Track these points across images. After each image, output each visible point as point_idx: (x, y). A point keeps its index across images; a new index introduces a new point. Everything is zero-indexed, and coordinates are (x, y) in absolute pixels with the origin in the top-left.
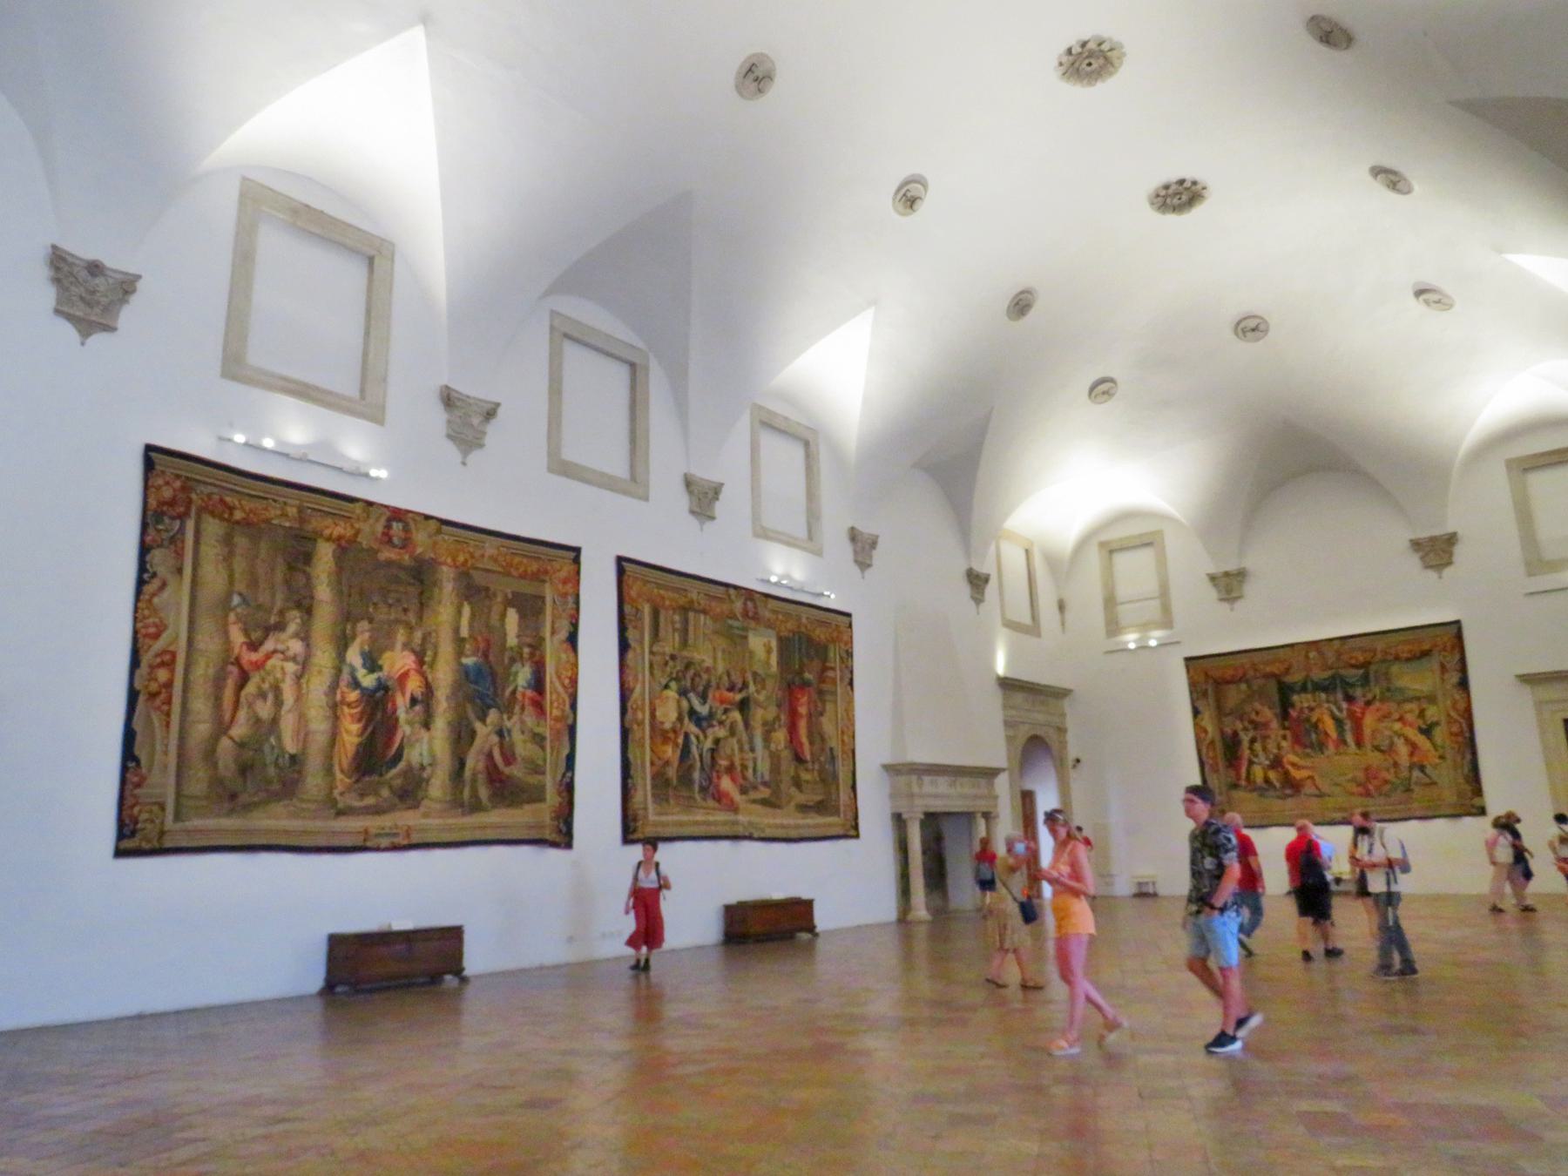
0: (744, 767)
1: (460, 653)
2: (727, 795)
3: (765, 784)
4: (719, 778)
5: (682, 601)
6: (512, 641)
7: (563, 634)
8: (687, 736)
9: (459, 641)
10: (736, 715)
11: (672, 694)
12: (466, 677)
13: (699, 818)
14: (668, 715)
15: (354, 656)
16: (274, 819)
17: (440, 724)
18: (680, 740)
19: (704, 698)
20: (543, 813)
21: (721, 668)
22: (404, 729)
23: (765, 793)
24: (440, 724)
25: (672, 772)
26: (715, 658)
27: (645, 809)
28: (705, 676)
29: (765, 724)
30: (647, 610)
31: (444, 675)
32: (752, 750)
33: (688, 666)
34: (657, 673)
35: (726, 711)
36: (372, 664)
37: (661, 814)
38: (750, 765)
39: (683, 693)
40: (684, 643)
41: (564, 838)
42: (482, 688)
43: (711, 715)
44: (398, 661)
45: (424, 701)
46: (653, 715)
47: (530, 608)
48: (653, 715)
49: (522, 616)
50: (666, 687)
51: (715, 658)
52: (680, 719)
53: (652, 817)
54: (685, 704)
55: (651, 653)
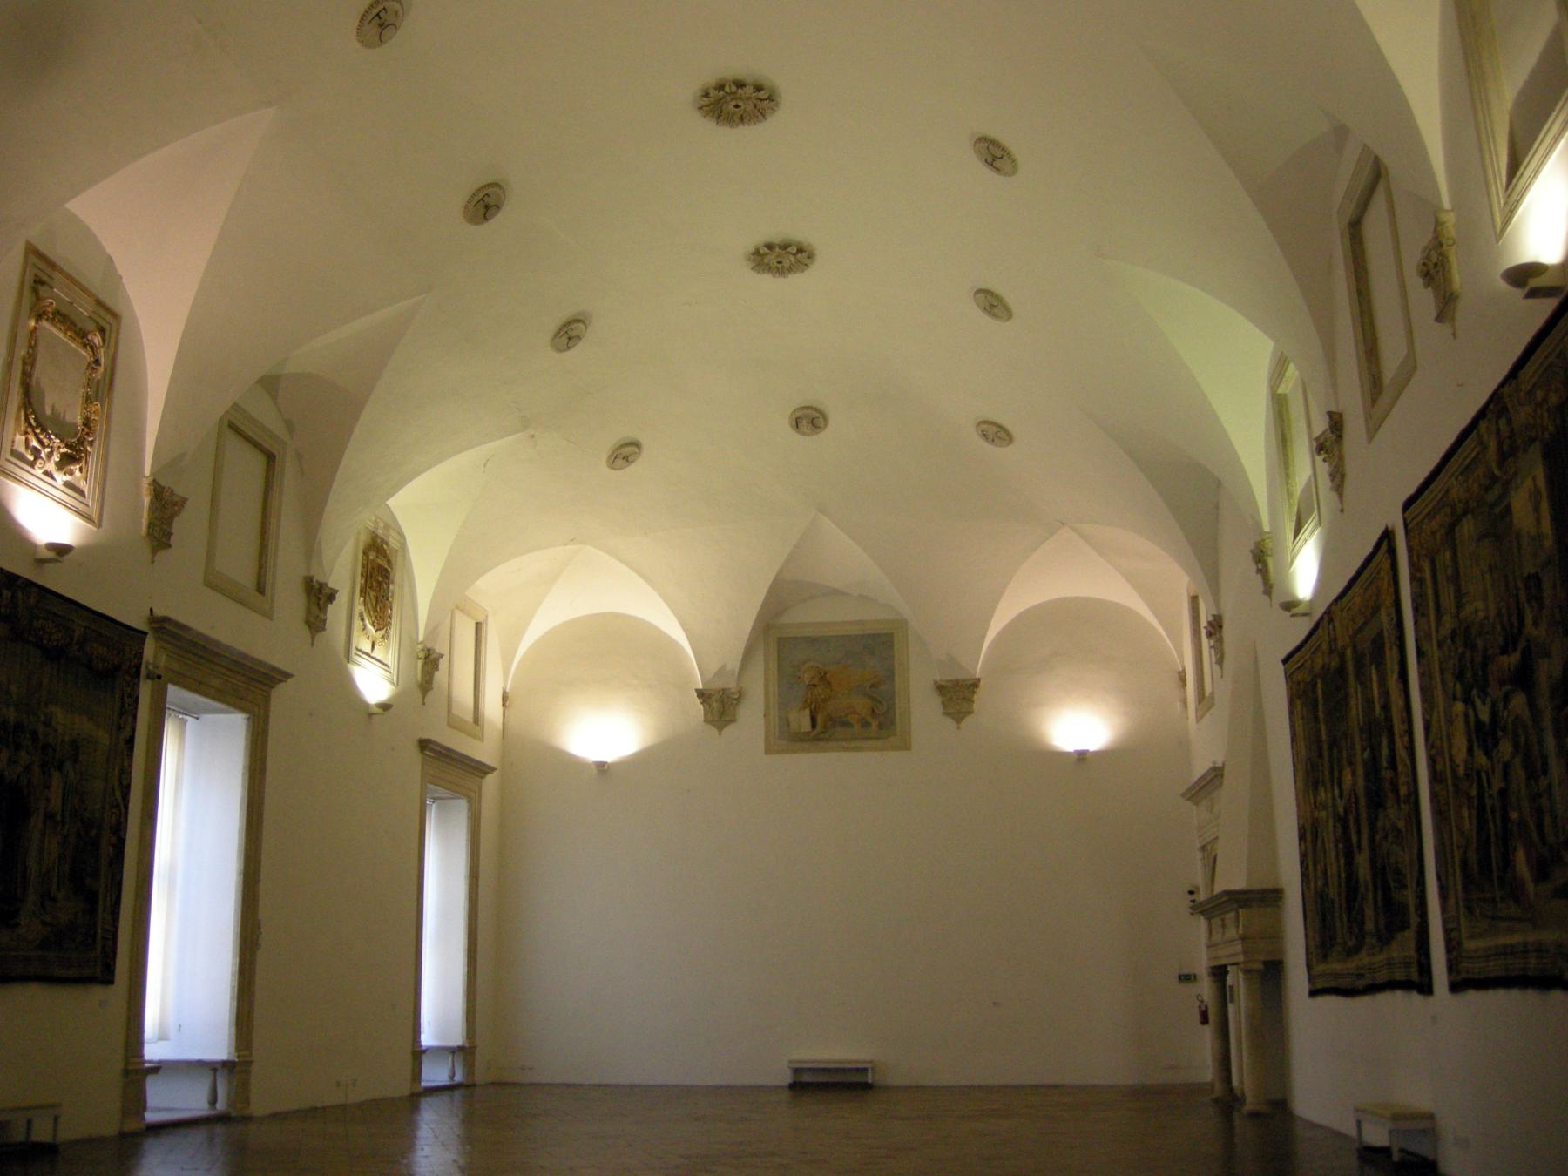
1: (1363, 750)
7: (1395, 675)
9: (1361, 730)
17: (1365, 843)
18: (1474, 793)
21: (1493, 612)
28: (1480, 643)
31: (1361, 781)
32: (1545, 772)
39: (1468, 700)
44: (1348, 778)
45: (1357, 820)
46: (1451, 760)
50: (1455, 698)
52: (1470, 751)
55: (1440, 646)
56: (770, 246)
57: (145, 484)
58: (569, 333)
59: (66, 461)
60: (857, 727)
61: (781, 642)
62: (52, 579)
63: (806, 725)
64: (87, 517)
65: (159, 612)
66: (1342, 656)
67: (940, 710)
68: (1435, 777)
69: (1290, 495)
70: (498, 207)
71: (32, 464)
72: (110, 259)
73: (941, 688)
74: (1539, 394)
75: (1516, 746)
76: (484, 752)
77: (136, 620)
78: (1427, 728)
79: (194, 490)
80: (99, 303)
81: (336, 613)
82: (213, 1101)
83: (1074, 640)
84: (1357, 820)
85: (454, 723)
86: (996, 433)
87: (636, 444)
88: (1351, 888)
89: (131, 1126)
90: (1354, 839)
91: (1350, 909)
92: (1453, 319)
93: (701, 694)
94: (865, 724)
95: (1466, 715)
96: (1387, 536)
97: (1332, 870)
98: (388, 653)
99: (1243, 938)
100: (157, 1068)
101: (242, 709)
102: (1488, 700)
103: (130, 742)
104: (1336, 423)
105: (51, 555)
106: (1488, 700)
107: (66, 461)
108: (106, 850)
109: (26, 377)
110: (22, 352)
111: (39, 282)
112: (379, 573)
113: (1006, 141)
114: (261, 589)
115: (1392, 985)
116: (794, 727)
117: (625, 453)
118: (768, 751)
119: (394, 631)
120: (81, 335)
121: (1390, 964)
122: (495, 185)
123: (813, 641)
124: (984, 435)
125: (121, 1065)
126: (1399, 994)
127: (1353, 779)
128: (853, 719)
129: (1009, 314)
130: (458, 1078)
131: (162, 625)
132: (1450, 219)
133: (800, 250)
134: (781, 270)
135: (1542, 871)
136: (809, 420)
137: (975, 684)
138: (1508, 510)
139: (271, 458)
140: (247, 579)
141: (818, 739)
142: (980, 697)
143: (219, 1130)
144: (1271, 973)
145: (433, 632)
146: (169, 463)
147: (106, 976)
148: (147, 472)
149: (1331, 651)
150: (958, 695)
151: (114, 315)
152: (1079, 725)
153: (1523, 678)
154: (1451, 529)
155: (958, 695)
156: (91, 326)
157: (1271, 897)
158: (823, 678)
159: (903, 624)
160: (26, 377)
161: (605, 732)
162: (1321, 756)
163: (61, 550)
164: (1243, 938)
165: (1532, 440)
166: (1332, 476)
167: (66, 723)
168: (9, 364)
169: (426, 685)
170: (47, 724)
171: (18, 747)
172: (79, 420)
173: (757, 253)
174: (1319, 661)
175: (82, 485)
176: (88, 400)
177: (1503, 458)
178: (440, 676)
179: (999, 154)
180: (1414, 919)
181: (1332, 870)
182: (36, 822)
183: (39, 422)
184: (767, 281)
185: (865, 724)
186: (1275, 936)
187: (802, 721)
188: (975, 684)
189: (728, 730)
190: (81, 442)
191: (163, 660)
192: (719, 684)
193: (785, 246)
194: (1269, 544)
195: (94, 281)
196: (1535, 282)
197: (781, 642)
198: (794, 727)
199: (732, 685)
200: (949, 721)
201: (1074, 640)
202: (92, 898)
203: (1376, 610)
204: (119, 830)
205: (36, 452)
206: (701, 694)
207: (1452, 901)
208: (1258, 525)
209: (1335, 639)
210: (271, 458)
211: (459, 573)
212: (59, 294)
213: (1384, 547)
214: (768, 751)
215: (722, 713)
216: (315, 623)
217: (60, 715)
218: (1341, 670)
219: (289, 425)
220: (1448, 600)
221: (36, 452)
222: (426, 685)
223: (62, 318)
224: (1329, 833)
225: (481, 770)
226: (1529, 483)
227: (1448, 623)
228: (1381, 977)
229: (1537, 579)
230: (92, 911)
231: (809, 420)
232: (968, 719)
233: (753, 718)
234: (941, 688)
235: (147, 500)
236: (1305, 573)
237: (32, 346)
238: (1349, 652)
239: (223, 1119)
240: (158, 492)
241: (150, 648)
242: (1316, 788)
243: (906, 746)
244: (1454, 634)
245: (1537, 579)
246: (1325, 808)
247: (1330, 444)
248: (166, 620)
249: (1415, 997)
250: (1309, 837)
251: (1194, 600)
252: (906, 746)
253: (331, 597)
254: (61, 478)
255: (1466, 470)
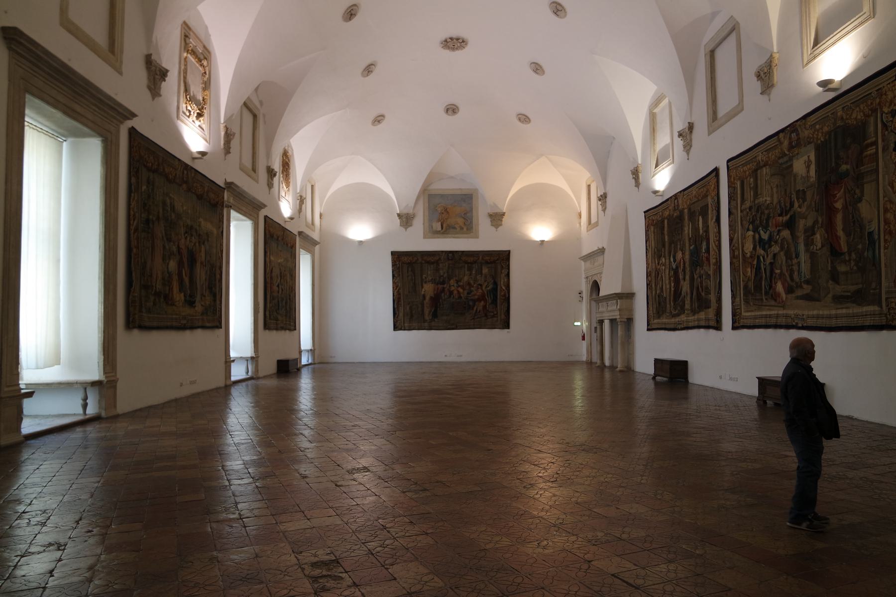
0: (791, 272)
1: (690, 246)
2: (779, 295)
3: (808, 282)
4: (776, 283)
5: (752, 166)
6: (701, 231)
8: (758, 258)
9: (690, 239)
10: (786, 233)
11: (751, 233)
12: (691, 255)
13: (764, 313)
14: (749, 247)
15: (672, 260)
16: (664, 320)
17: (687, 277)
18: (755, 262)
19: (766, 228)
20: (711, 313)
21: (775, 201)
22: (682, 282)
23: (807, 289)
24: (687, 277)
25: (751, 285)
26: (772, 196)
27: (740, 309)
28: (766, 212)
29: (806, 231)
30: (739, 183)
31: (687, 257)
32: (797, 256)
33: (757, 211)
34: (744, 222)
35: (779, 231)
36: (675, 261)
37: (748, 311)
38: (795, 268)
39: (755, 230)
40: (756, 195)
41: (718, 327)
42: (697, 260)
43: (771, 238)
44: (679, 255)
45: (684, 270)
46: (743, 250)
47: (704, 212)
48: (743, 250)
49: (703, 218)
50: (748, 230)
51: (772, 196)
52: (755, 248)
53: (744, 314)
54: (757, 236)
55: (741, 211)
56: (451, 39)
57: (222, 127)
58: (368, 70)
59: (199, 115)
60: (458, 229)
61: (430, 196)
62: (199, 166)
63: (439, 228)
64: (206, 140)
65: (229, 180)
66: (682, 212)
67: (490, 223)
68: (733, 257)
69: (654, 151)
70: (355, 15)
71: (189, 117)
72: (207, 27)
73: (490, 216)
74: (817, 127)
75: (782, 248)
76: (315, 236)
77: (221, 183)
78: (731, 240)
79: (235, 129)
80: (204, 47)
81: (276, 179)
82: (247, 372)
83: (540, 199)
84: (684, 270)
85: (307, 226)
86: (524, 119)
87: (383, 116)
88: (677, 293)
89: (228, 383)
90: (681, 277)
91: (675, 301)
92: (769, 95)
93: (399, 215)
94: (462, 228)
95: (754, 237)
96: (716, 171)
97: (666, 286)
98: (290, 197)
99: (620, 310)
100: (233, 361)
101: (251, 219)
102: (768, 233)
103: (222, 232)
104: (691, 127)
105: (200, 156)
106: (768, 233)
107: (199, 115)
108: (218, 276)
109: (185, 78)
110: (183, 67)
111: (186, 36)
112: (286, 165)
113: (563, 4)
114: (254, 170)
115: (699, 327)
116: (434, 228)
117: (378, 120)
118: (425, 237)
119: (291, 188)
120: (200, 60)
121: (699, 320)
122: (355, 5)
123: (442, 196)
124: (520, 119)
125: (224, 360)
126: (702, 330)
127: (683, 256)
128: (457, 226)
129: (543, 72)
130: (310, 361)
131: (230, 186)
132: (776, 56)
133: (463, 41)
134: (453, 49)
135: (790, 290)
136: (452, 110)
137: (504, 214)
138: (791, 166)
139: (255, 116)
140: (250, 167)
141: (443, 233)
142: (505, 219)
143: (250, 382)
144: (629, 322)
145: (301, 190)
146: (228, 120)
147: (219, 327)
148: (222, 121)
149: (675, 210)
150: (497, 218)
151: (209, 52)
152: (541, 231)
153: (790, 225)
154: (756, 170)
155: (497, 218)
156: (202, 57)
157: (630, 296)
158: (446, 210)
159: (476, 190)
160: (185, 78)
161: (360, 230)
162: (664, 246)
163: (203, 154)
164: (620, 310)
165: (810, 143)
166: (685, 147)
167: (206, 226)
168: (180, 73)
169: (300, 210)
170: (200, 226)
171: (192, 235)
172: (201, 99)
173: (446, 41)
174: (667, 213)
175: (204, 126)
176: (204, 89)
177: (791, 147)
178: (304, 206)
179: (560, 8)
180: (714, 304)
181: (666, 286)
182: (198, 264)
183: (192, 99)
184: (447, 52)
185: (462, 228)
186: (631, 310)
187: (437, 226)
188: (504, 214)
189: (409, 229)
190: (203, 108)
191: (231, 200)
192: (405, 211)
193: (458, 39)
194: (640, 169)
195: (202, 37)
196: (830, 86)
197: (430, 196)
198: (434, 228)
199: (411, 212)
200: (493, 229)
201: (540, 199)
202: (215, 296)
203: (706, 196)
204: (221, 268)
205: (190, 111)
206: (399, 215)
207: (738, 299)
208: (635, 160)
209: (678, 205)
210: (255, 116)
211: (313, 165)
212: (192, 42)
213: (714, 174)
214: (425, 237)
215: (407, 223)
216: (270, 185)
217: (203, 223)
218: (681, 218)
219: (261, 103)
220: (750, 195)
221: (190, 111)
222: (300, 210)
223: (194, 53)
224: (666, 275)
225: (315, 243)
226: (805, 158)
227: (748, 204)
228: (696, 324)
229: (804, 192)
230: (215, 301)
231: (452, 110)
232: (500, 228)
233: (419, 224)
234: (490, 216)
235: (223, 133)
236: (662, 180)
237: (186, 65)
238: (686, 211)
239: (251, 378)
240: (227, 129)
241: (226, 195)
242: (659, 257)
243: (477, 237)
244: (750, 208)
245: (804, 192)
246: (664, 265)
247: (687, 134)
248: (232, 183)
249: (712, 332)
250: (653, 275)
251: (589, 186)
252: (477, 237)
253: (275, 175)
254: (197, 123)
255: (768, 151)
